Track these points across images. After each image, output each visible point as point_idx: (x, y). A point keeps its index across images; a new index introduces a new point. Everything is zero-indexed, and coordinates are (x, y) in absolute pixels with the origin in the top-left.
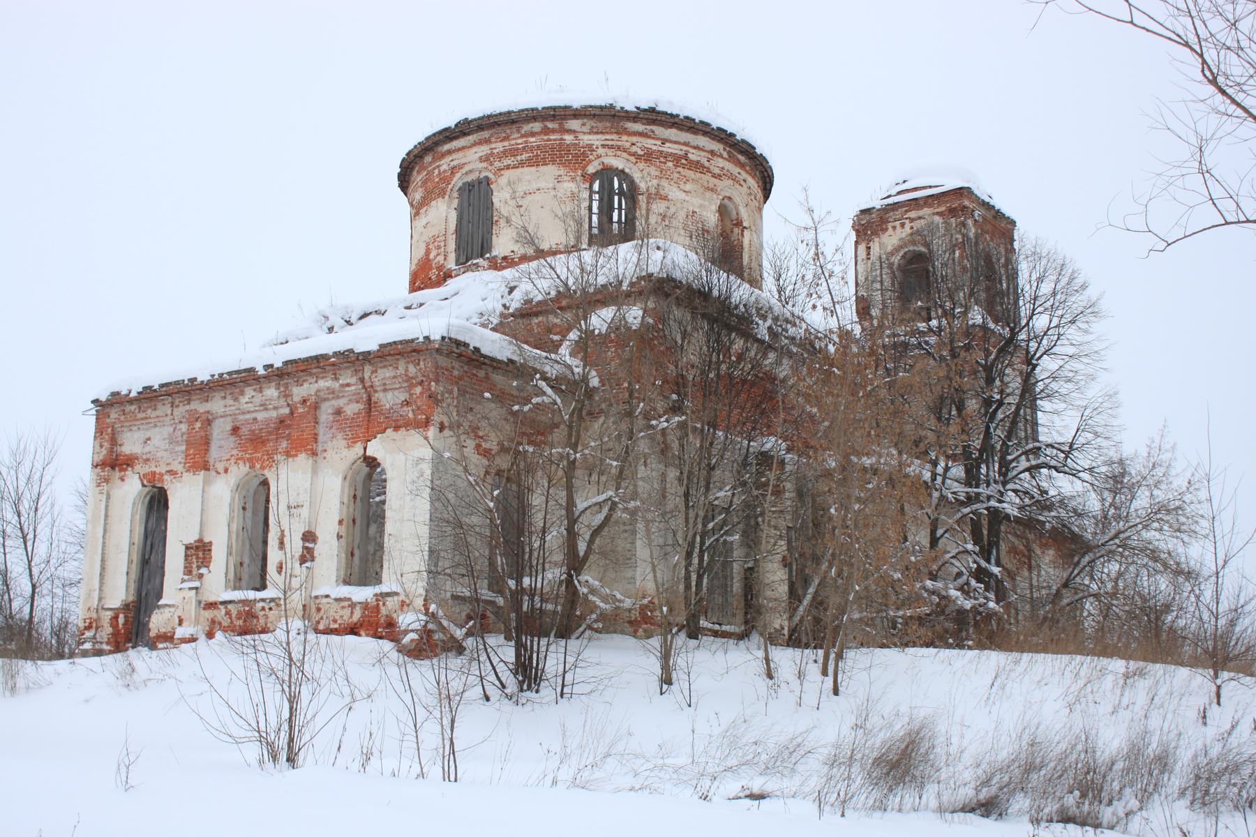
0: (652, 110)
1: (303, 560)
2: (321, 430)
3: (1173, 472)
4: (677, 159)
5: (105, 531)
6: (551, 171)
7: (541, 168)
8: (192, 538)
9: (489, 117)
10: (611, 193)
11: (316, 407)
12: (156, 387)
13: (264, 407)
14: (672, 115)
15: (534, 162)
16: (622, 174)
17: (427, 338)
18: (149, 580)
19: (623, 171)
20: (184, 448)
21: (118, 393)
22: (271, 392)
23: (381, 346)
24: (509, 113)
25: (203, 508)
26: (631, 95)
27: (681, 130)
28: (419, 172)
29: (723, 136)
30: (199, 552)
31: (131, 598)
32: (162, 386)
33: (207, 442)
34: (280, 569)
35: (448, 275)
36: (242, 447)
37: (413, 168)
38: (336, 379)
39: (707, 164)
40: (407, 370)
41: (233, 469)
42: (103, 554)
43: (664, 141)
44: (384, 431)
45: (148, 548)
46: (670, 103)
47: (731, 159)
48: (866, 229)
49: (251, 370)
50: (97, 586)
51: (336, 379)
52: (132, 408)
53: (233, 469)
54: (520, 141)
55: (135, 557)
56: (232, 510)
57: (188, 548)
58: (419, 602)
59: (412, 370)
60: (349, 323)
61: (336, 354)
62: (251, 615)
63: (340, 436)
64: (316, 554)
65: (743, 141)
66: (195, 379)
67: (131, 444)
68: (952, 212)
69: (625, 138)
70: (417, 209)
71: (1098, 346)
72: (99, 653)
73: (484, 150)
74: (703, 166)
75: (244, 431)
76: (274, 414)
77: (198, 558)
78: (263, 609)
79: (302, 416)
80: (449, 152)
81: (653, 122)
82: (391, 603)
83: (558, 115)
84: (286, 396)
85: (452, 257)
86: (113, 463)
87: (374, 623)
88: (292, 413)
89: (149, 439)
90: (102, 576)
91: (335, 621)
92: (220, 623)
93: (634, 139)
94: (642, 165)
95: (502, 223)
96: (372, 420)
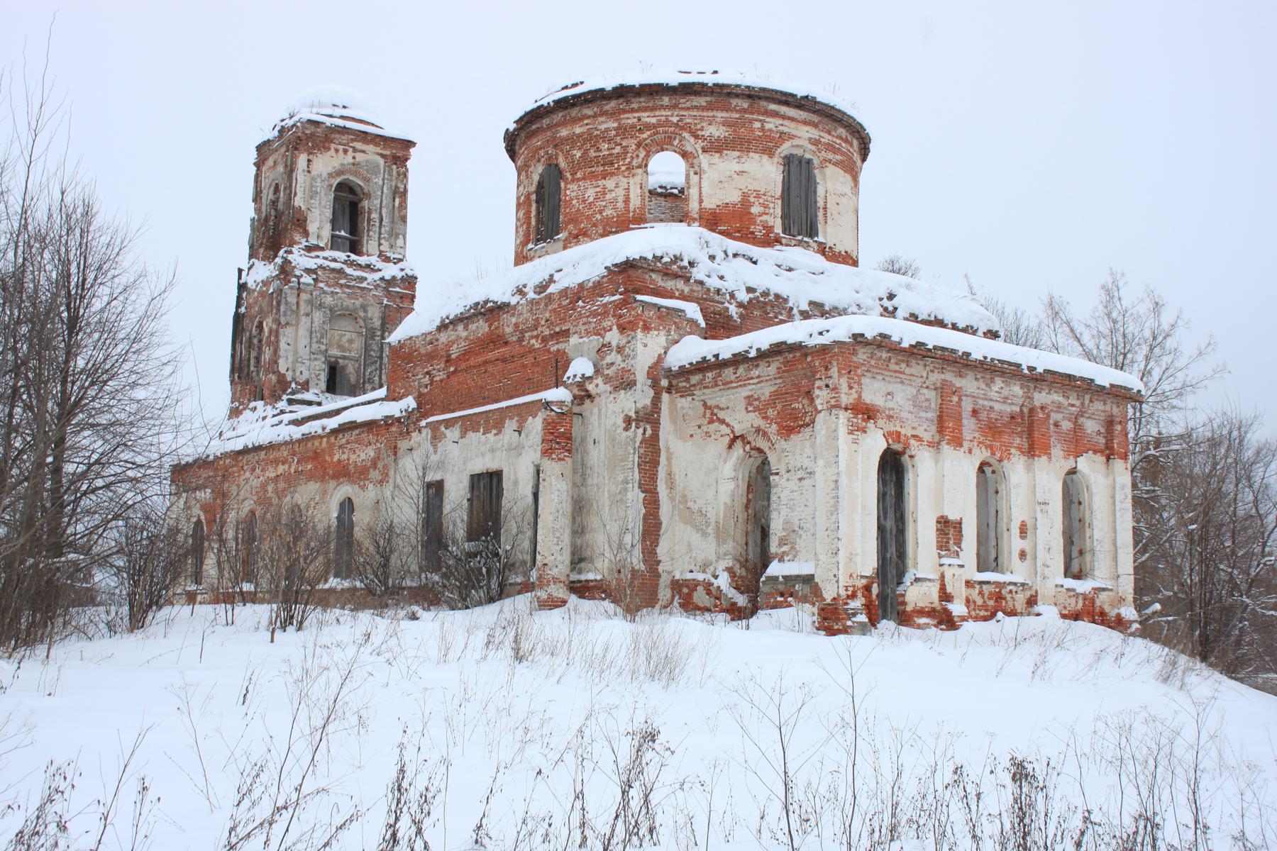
9: (832, 108)
22: (1017, 389)
23: (1112, 385)
32: (935, 348)
41: (976, 451)
53: (976, 451)
58: (1130, 598)
59: (1115, 410)
62: (999, 597)
67: (873, 392)
73: (814, 133)
75: (983, 416)
76: (1008, 409)
78: (1011, 592)
80: (784, 117)
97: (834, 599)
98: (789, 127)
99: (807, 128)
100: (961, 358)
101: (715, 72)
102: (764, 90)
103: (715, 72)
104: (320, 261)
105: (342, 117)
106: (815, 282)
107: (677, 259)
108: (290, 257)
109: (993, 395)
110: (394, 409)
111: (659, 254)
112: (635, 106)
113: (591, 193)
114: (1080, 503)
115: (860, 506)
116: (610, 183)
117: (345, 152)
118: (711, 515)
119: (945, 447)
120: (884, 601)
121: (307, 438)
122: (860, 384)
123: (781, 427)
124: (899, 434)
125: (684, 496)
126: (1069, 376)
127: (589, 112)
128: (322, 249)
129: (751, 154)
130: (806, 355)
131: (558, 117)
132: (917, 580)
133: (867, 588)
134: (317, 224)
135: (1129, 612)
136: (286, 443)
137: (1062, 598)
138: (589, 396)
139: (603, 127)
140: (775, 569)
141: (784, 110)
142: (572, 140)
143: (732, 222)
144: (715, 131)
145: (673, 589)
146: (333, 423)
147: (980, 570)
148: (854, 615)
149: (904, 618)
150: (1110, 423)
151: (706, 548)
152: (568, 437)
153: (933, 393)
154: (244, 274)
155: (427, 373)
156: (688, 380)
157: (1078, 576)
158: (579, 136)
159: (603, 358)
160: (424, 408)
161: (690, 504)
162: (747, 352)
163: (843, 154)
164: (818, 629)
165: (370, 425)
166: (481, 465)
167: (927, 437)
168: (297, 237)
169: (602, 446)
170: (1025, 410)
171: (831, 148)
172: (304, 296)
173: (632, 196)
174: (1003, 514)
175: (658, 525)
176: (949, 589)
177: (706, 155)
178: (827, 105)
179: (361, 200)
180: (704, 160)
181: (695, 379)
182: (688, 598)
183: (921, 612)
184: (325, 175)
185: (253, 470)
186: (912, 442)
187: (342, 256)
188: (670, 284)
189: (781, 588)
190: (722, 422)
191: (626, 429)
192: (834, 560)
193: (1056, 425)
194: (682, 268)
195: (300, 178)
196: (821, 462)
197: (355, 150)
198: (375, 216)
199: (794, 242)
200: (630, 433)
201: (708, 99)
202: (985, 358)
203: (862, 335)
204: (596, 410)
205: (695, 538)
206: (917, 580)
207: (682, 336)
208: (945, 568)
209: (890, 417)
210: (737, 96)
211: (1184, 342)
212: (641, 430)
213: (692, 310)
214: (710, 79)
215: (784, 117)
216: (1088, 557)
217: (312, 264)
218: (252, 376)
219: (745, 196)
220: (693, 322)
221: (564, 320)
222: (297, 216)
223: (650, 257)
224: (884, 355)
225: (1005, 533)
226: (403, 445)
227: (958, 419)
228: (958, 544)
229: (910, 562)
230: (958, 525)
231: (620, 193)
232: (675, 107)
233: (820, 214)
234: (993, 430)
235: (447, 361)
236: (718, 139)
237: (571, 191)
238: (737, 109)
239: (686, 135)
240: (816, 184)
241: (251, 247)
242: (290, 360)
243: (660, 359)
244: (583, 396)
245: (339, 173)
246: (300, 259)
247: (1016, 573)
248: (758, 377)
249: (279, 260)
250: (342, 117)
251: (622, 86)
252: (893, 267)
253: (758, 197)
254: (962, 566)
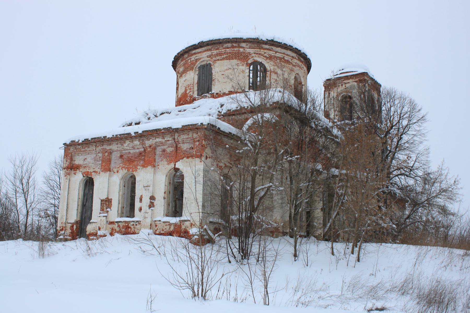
0: (272, 41)
1: (150, 207)
2: (157, 157)
3: (448, 177)
4: (280, 59)
5: (68, 193)
6: (234, 62)
7: (231, 61)
8: (104, 197)
10: (257, 71)
11: (155, 149)
12: (90, 139)
13: (133, 148)
14: (279, 43)
15: (228, 58)
16: (261, 64)
17: (202, 124)
18: (86, 213)
19: (261, 63)
20: (100, 162)
21: (74, 141)
22: (137, 142)
23: (183, 126)
24: (219, 39)
25: (108, 186)
26: (265, 35)
27: (282, 48)
28: (182, 61)
29: (297, 51)
30: (107, 203)
31: (78, 219)
32: (92, 139)
33: (110, 161)
34: (140, 209)
35: (194, 100)
36: (124, 163)
37: (179, 59)
38: (164, 138)
39: (291, 61)
40: (193, 136)
41: (121, 171)
42: (68, 202)
43: (276, 52)
44: (183, 159)
45: (85, 201)
46: (279, 38)
47: (299, 59)
48: (328, 86)
49: (129, 134)
50: (65, 214)
51: (164, 138)
52: (80, 147)
53: (121, 171)
54: (223, 50)
55: (80, 204)
56: (120, 187)
57: (102, 201)
58: (198, 224)
59: (195, 135)
60: (156, 116)
61: (164, 129)
62: (128, 227)
63: (165, 160)
64: (155, 204)
65: (304, 53)
66: (106, 137)
67: (78, 160)
68: (360, 81)
69: (262, 50)
70: (180, 75)
71: (423, 132)
72: (66, 240)
73: (209, 53)
74: (289, 62)
75: (125, 157)
76: (138, 151)
77: (106, 205)
78: (133, 225)
79: (149, 152)
80: (195, 54)
81: (272, 45)
82: (187, 224)
83: (237, 41)
84: (143, 144)
85: (196, 93)
86: (72, 168)
87: (180, 232)
88: (145, 151)
89: (86, 159)
90: (67, 210)
91: (163, 230)
92: (115, 230)
93: (266, 51)
94: (268, 61)
95: (216, 81)
96: (177, 154)
99: (205, 53)
105: (341, 74)
106: (193, 112)
149: (88, 237)
202: (113, 136)
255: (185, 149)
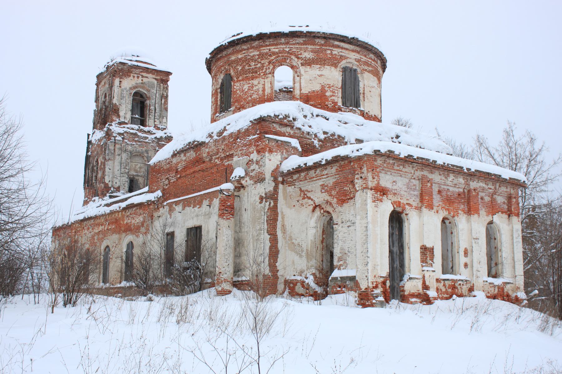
9: (367, 43)
22: (461, 180)
23: (510, 178)
32: (418, 158)
36: (443, 201)
54: (370, 61)
58: (522, 287)
62: (454, 287)
67: (386, 181)
73: (358, 56)
75: (444, 194)
76: (457, 190)
78: (460, 284)
80: (342, 48)
89: (394, 182)
91: (489, 293)
92: (441, 290)
97: (366, 289)
98: (345, 53)
99: (354, 54)
100: (432, 163)
101: (307, 26)
102: (332, 34)
103: (307, 26)
104: (125, 130)
105: (136, 61)
107: (287, 116)
108: (111, 127)
109: (449, 183)
110: (151, 197)
111: (277, 114)
112: (268, 43)
113: (246, 87)
114: (495, 239)
115: (379, 240)
116: (255, 82)
117: (138, 77)
118: (304, 246)
119: (424, 210)
120: (393, 289)
121: (112, 213)
122: (378, 176)
123: (339, 200)
124: (399, 202)
125: (291, 237)
126: (488, 173)
127: (245, 47)
128: (126, 124)
129: (326, 66)
130: (350, 162)
131: (230, 50)
132: (410, 278)
133: (384, 283)
134: (124, 112)
135: (522, 295)
136: (103, 215)
137: (487, 288)
138: (243, 187)
139: (252, 54)
140: (336, 274)
141: (342, 44)
142: (237, 61)
143: (316, 99)
144: (308, 55)
145: (285, 285)
146: (123, 205)
147: (444, 273)
148: (377, 297)
149: (404, 299)
150: (510, 198)
151: (302, 263)
152: (233, 208)
153: (418, 182)
154: (90, 136)
155: (167, 178)
156: (292, 177)
157: (495, 276)
158: (240, 59)
159: (249, 167)
160: (165, 197)
161: (294, 241)
162: (321, 161)
163: (373, 67)
164: (358, 305)
165: (140, 205)
166: (192, 223)
167: (414, 204)
168: (114, 118)
169: (249, 212)
170: (466, 191)
171: (366, 63)
172: (117, 146)
173: (266, 88)
174: (455, 244)
175: (277, 252)
176: (427, 283)
177: (303, 67)
178: (364, 42)
179: (146, 100)
180: (302, 69)
181: (295, 177)
182: (294, 290)
183: (413, 295)
184: (128, 88)
185: (88, 229)
186: (407, 207)
187: (136, 127)
188: (283, 130)
189: (339, 283)
190: (309, 198)
191: (261, 203)
192: (366, 268)
193: (482, 198)
194: (289, 121)
195: (116, 89)
196: (358, 217)
197: (143, 76)
198: (152, 108)
199: (348, 110)
200: (262, 205)
201: (304, 39)
202: (444, 163)
203: (379, 151)
204: (246, 194)
205: (296, 258)
206: (410, 278)
207: (289, 156)
208: (425, 272)
209: (395, 194)
210: (318, 37)
211: (547, 158)
212: (268, 203)
213: (295, 143)
214: (305, 30)
215: (342, 48)
216: (500, 266)
217: (121, 130)
218: (94, 185)
219: (323, 87)
220: (295, 148)
221: (230, 149)
222: (114, 108)
223: (273, 115)
224: (391, 162)
225: (457, 254)
226: (156, 214)
227: (431, 195)
228: (432, 261)
229: (406, 269)
230: (432, 250)
231: (261, 86)
232: (287, 43)
233: (361, 96)
234: (449, 201)
235: (176, 172)
236: (309, 59)
237: (236, 86)
238: (320, 44)
239: (293, 57)
240: (359, 81)
241: (94, 124)
242: (111, 177)
243: (278, 167)
244: (240, 187)
245: (135, 87)
246: (115, 128)
247: (462, 275)
248: (327, 174)
249: (105, 129)
250: (136, 61)
251: (261, 33)
252: (399, 123)
253: (329, 87)
254: (434, 271)
255: (499, 202)
